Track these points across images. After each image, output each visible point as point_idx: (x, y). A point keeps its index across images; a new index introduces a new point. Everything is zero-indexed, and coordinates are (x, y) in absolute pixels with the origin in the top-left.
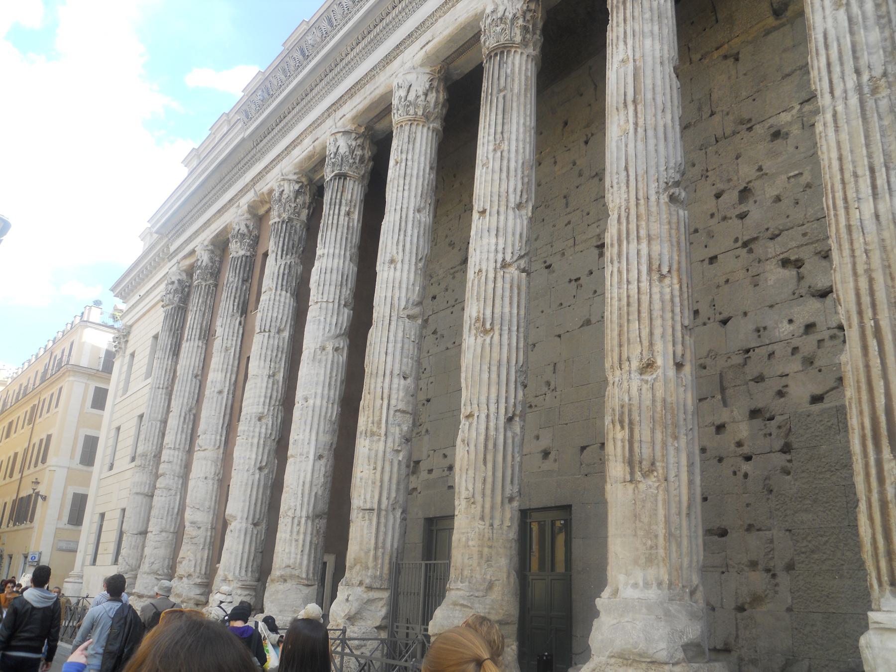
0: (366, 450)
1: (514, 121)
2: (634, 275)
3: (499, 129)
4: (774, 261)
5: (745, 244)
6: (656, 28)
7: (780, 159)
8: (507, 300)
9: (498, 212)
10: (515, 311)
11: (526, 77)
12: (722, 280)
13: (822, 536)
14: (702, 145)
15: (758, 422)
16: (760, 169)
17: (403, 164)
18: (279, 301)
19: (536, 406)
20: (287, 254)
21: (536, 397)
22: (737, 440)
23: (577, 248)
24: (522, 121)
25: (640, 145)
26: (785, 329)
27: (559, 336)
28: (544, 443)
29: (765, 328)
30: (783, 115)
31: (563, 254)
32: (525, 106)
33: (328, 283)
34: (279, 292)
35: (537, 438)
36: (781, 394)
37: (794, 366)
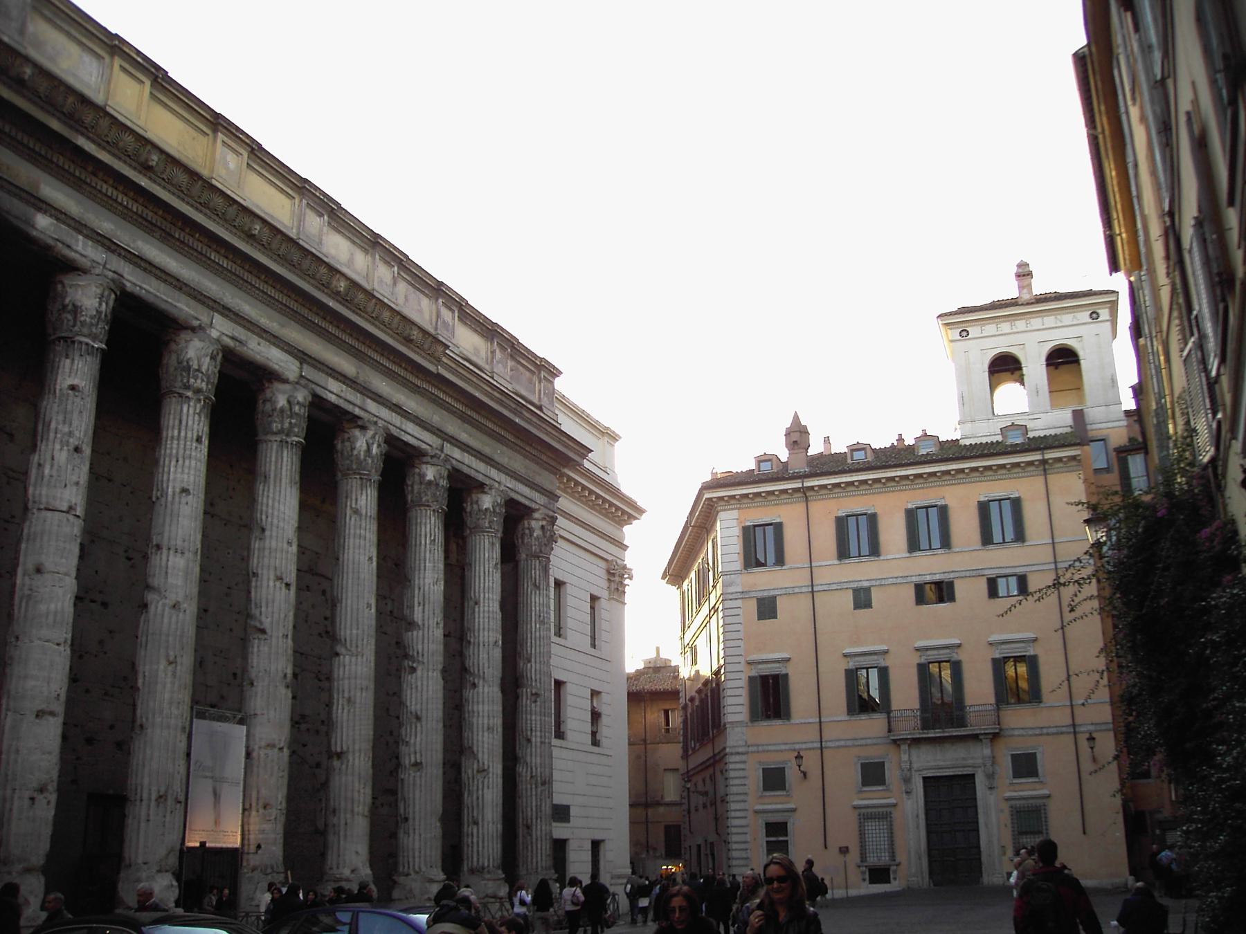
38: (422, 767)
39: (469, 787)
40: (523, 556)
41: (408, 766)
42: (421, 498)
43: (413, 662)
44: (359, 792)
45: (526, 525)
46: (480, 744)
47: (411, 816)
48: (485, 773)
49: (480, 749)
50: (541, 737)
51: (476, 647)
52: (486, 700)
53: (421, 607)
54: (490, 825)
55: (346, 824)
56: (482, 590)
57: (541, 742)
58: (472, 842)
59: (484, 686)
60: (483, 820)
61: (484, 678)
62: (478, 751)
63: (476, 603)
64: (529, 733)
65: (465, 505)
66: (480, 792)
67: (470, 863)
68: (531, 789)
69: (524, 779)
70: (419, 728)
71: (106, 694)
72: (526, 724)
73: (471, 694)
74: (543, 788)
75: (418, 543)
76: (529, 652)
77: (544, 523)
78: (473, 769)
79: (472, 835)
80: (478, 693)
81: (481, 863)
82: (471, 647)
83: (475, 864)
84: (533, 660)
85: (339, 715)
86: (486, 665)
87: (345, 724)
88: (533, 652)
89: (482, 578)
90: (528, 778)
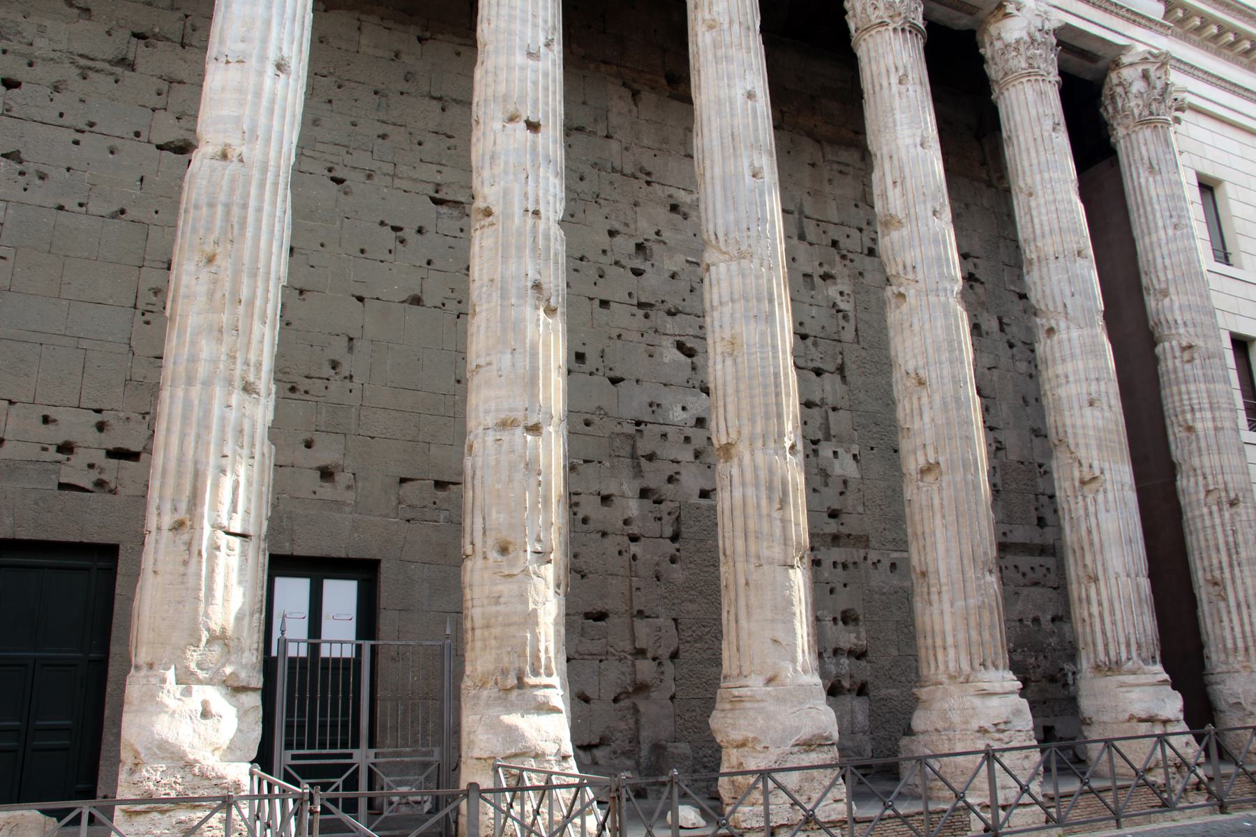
0: (232, 415)
4: (671, 339)
5: (640, 305)
7: (679, 237)
12: (614, 334)
13: (704, 626)
14: (596, 164)
15: (648, 503)
16: (658, 233)
19: (306, 392)
21: (307, 377)
22: (626, 517)
23: (397, 182)
26: (677, 415)
27: (361, 299)
28: (325, 454)
29: (658, 405)
30: (683, 192)
31: (369, 177)
35: (309, 445)
36: (671, 480)
37: (686, 455)
38: (941, 473)
39: (1070, 510)
40: (1121, 132)
41: (914, 473)
42: (868, 16)
43: (900, 285)
44: (769, 515)
45: (1115, 81)
46: (1080, 431)
47: (931, 568)
48: (1094, 486)
49: (1081, 441)
50: (1214, 419)
51: (1044, 263)
52: (1078, 351)
53: (898, 190)
54: (1123, 578)
55: (747, 584)
56: (1035, 168)
57: (1216, 429)
58: (1090, 615)
59: (1068, 328)
60: (1105, 570)
61: (1066, 313)
62: (1077, 445)
63: (1031, 195)
64: (1189, 416)
65: (982, 51)
66: (1093, 519)
67: (1092, 656)
68: (1211, 513)
69: (1194, 498)
70: (925, 400)
71: (293, 389)
72: (1181, 400)
73: (1048, 349)
74: (1234, 510)
75: (877, 88)
76: (1162, 278)
77: (1145, 67)
78: (1073, 479)
79: (1089, 602)
80: (1060, 342)
81: (1112, 654)
82: (1035, 268)
83: (1102, 656)
84: (1172, 290)
85: (719, 374)
86: (1068, 293)
87: (730, 390)
88: (1170, 276)
89: (1033, 151)
90: (1202, 495)
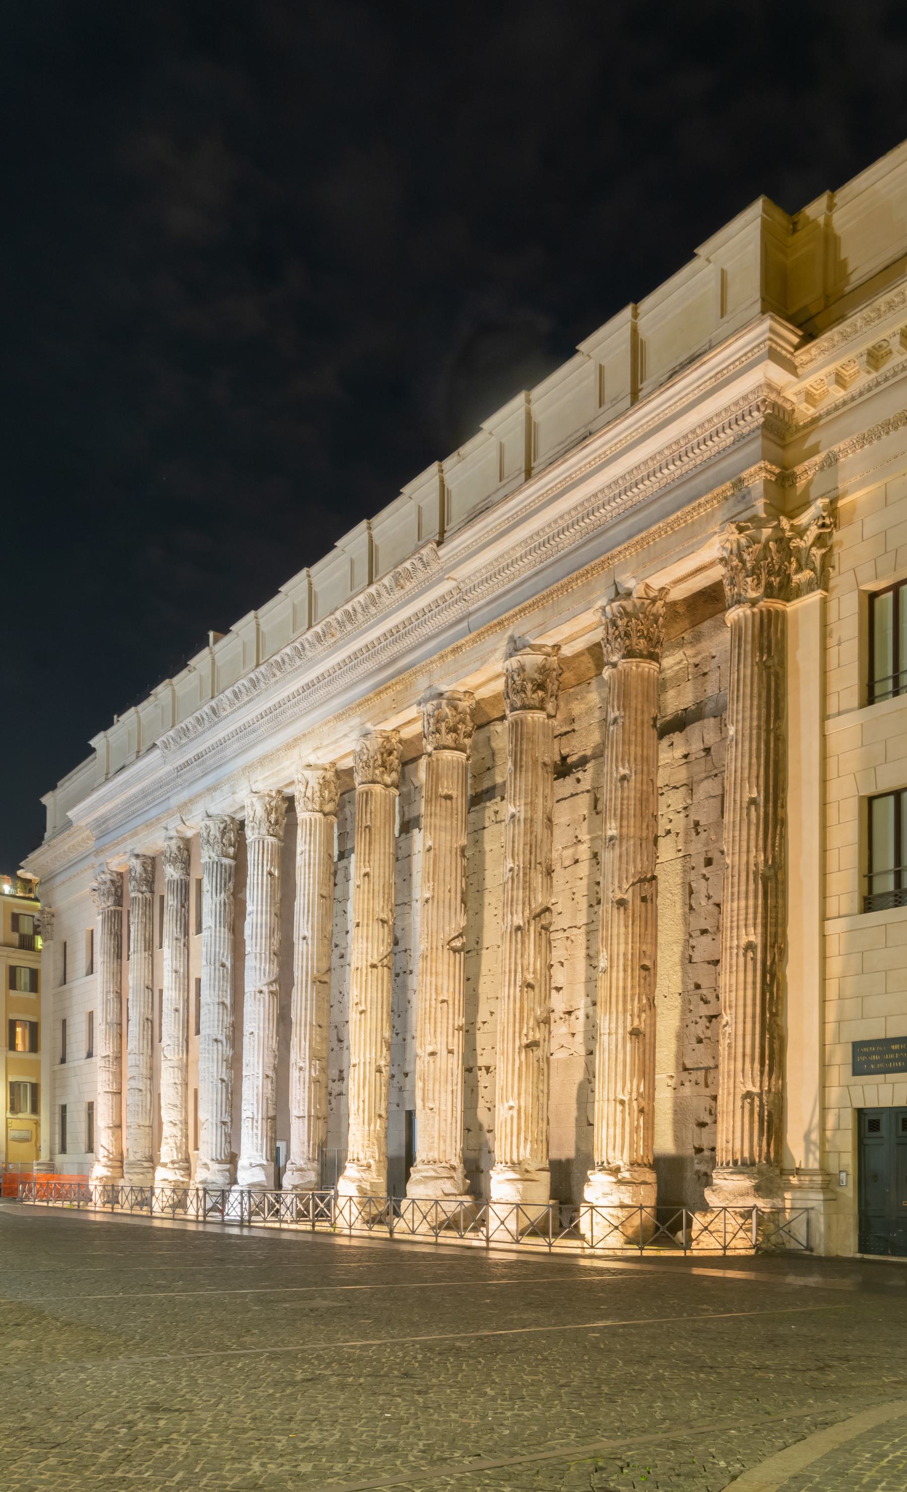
1: (377, 851)
2: (428, 997)
3: (367, 859)
6: (449, 823)
8: (374, 988)
9: (368, 925)
10: (380, 995)
11: (385, 811)
17: (307, 854)
18: (220, 937)
20: (221, 893)
24: (382, 851)
25: (435, 913)
32: (385, 838)
33: (259, 937)
34: (218, 929)
